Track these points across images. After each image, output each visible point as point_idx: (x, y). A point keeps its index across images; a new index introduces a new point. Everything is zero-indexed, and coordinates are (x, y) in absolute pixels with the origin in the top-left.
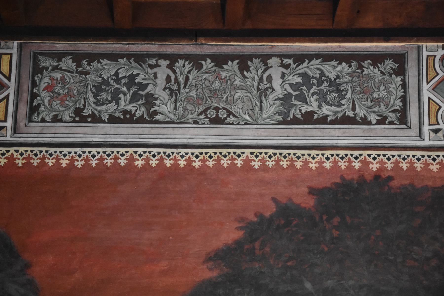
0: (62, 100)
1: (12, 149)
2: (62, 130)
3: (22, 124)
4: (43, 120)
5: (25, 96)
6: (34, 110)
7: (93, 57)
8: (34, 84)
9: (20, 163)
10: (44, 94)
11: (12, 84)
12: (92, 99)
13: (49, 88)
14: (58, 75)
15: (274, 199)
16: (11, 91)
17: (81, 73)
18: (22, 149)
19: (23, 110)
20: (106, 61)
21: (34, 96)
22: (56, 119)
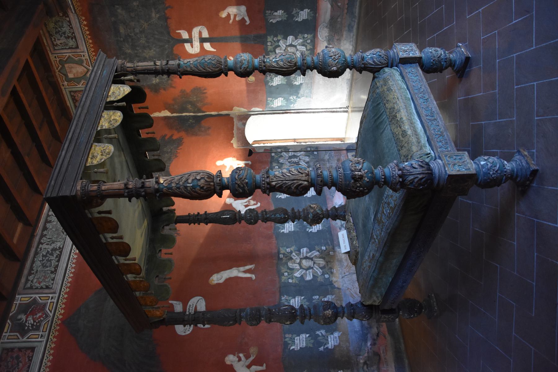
0: (46, 278)
1: (62, 293)
2: (58, 277)
3: (52, 291)
4: (53, 284)
5: (41, 291)
6: (47, 287)
7: (31, 268)
8: (37, 288)
9: (68, 290)
10: (42, 284)
11: (34, 296)
12: (48, 268)
13: (39, 283)
14: (35, 280)
16: (37, 296)
17: (37, 272)
18: (63, 290)
19: (47, 291)
20: (34, 265)
21: (42, 288)
22: (53, 280)
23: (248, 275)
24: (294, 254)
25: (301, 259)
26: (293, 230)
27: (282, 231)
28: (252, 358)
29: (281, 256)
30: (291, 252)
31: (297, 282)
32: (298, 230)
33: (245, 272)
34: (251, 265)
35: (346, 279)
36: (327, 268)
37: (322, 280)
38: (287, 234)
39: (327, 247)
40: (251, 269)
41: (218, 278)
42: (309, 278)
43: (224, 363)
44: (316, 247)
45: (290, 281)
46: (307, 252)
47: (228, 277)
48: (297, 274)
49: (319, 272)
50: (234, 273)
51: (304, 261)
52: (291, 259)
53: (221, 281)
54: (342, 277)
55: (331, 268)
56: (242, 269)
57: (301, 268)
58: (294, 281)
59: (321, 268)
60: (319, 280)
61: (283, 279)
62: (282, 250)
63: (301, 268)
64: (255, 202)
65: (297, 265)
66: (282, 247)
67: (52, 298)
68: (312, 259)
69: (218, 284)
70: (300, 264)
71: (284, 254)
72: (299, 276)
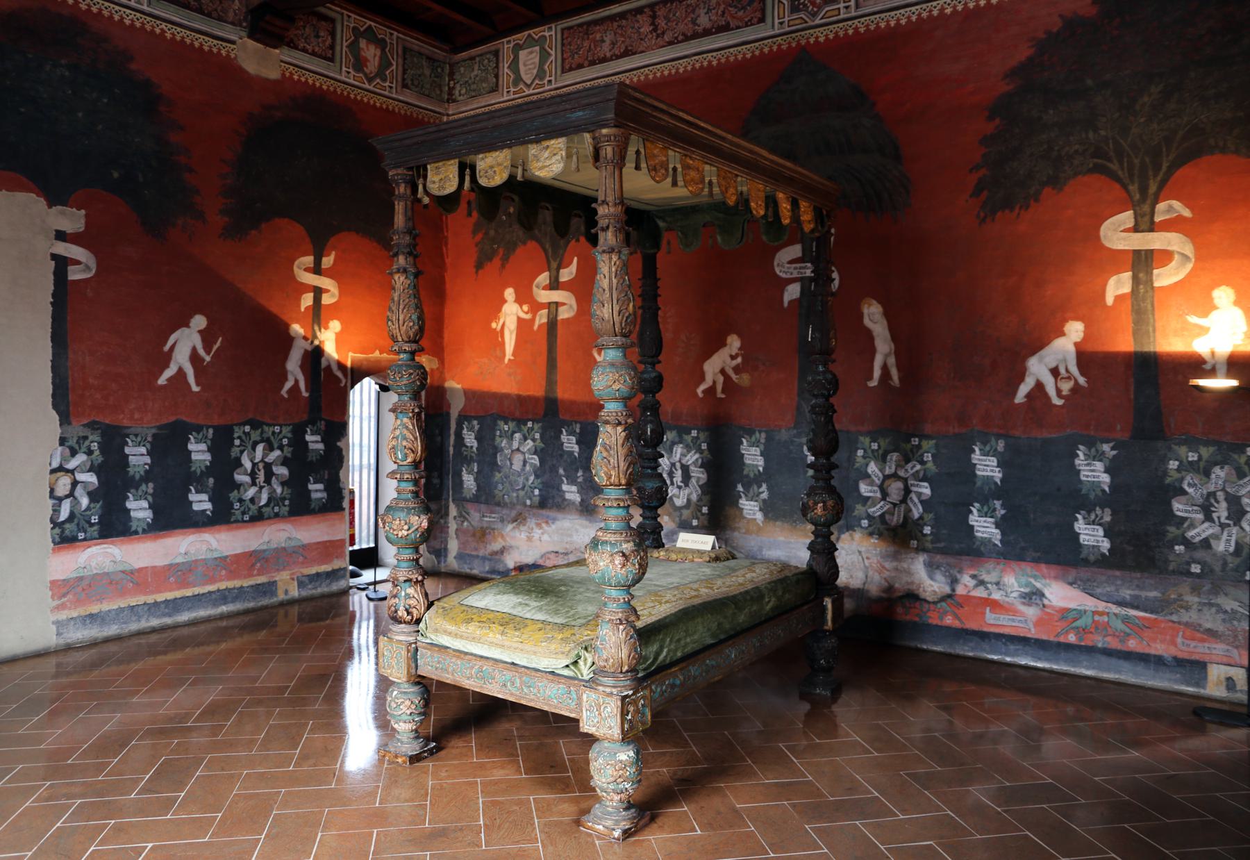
15: (1060, 16)
23: (877, 373)
24: (918, 467)
25: (905, 480)
26: (978, 473)
27: (977, 449)
28: (734, 376)
29: (915, 441)
30: (922, 463)
31: (857, 465)
32: (979, 484)
33: (885, 368)
34: (900, 379)
35: (856, 558)
36: (882, 527)
37: (856, 513)
38: (970, 459)
39: (929, 538)
40: (891, 378)
41: (873, 315)
42: (864, 489)
43: (728, 334)
44: (931, 516)
45: (860, 453)
46: (919, 495)
47: (875, 334)
48: (873, 468)
49: (876, 510)
50: (883, 346)
51: (900, 485)
52: (907, 461)
53: (867, 322)
54: (860, 552)
55: (880, 535)
56: (892, 361)
57: (886, 477)
58: (859, 460)
59: (882, 516)
60: (859, 507)
61: (866, 440)
62: (928, 444)
63: (886, 477)
64: (1064, 393)
65: (893, 470)
66: (937, 445)
67: (847, 7)
68: (904, 501)
69: (860, 316)
70: (895, 476)
71: (919, 447)
72: (869, 471)
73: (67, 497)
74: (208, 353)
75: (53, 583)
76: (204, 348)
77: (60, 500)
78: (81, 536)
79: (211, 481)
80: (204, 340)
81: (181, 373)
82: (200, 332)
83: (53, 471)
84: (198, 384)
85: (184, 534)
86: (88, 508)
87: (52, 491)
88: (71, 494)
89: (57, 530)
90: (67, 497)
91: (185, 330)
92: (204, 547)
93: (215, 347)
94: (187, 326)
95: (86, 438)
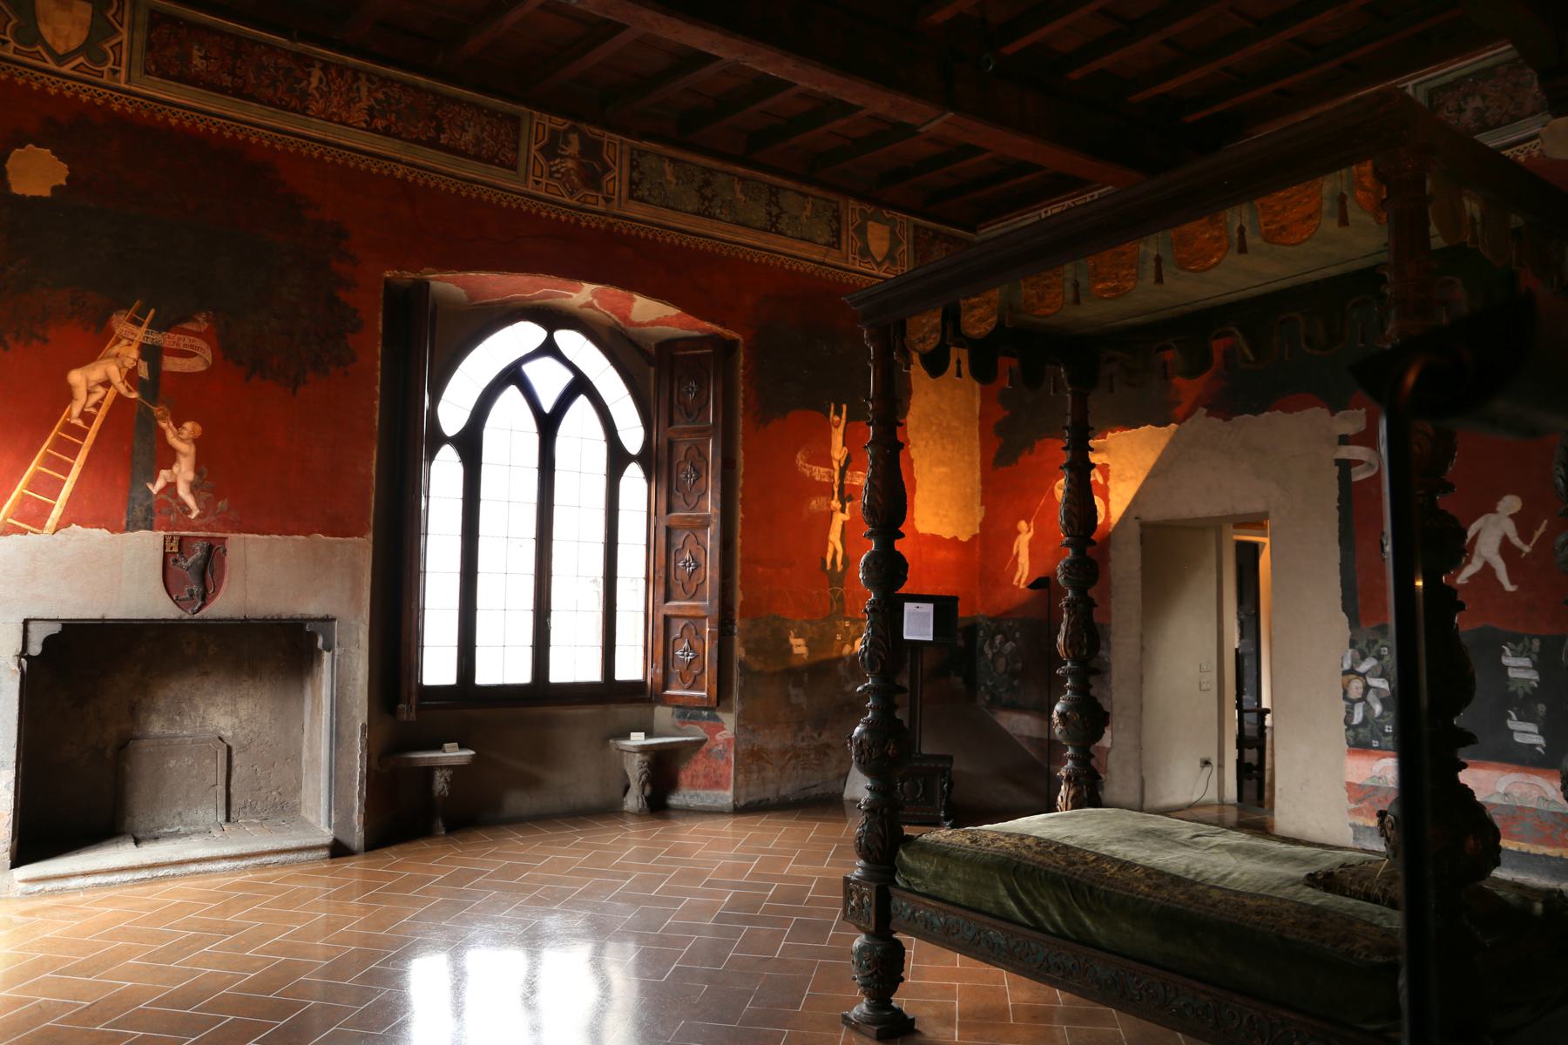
73: (1359, 700)
74: (1527, 542)
75: (1350, 786)
76: (1520, 536)
77: (1353, 702)
78: (1375, 744)
79: (1542, 708)
80: (1518, 527)
81: (1487, 569)
82: (1511, 516)
83: (1345, 673)
84: (1512, 582)
85: (1503, 769)
86: (1381, 716)
87: (1345, 692)
88: (1363, 699)
89: (1351, 733)
90: (1359, 700)
91: (1492, 517)
92: (1535, 794)
93: (1537, 534)
94: (1493, 511)
95: (1375, 642)
